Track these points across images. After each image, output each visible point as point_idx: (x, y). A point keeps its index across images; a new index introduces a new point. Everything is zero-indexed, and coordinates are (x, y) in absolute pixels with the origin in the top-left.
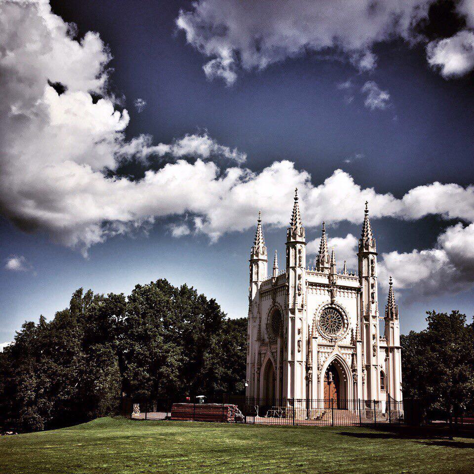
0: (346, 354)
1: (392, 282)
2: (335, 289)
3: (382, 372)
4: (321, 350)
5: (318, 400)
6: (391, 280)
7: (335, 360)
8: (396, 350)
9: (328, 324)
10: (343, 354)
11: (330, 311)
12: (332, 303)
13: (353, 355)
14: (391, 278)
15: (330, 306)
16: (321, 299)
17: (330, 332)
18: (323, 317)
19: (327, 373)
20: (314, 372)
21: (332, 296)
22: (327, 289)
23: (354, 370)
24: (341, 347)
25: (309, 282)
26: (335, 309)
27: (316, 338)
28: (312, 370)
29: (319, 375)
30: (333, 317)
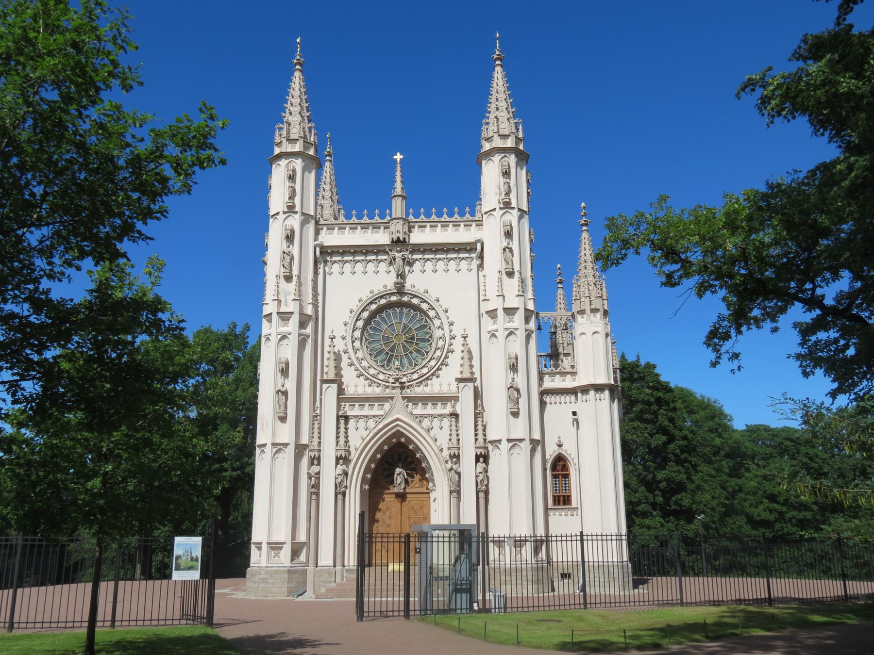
0: (430, 416)
8: (592, 392)
10: (416, 416)
12: (400, 290)
15: (394, 298)
21: (401, 276)
23: (456, 457)
26: (409, 305)
28: (319, 464)
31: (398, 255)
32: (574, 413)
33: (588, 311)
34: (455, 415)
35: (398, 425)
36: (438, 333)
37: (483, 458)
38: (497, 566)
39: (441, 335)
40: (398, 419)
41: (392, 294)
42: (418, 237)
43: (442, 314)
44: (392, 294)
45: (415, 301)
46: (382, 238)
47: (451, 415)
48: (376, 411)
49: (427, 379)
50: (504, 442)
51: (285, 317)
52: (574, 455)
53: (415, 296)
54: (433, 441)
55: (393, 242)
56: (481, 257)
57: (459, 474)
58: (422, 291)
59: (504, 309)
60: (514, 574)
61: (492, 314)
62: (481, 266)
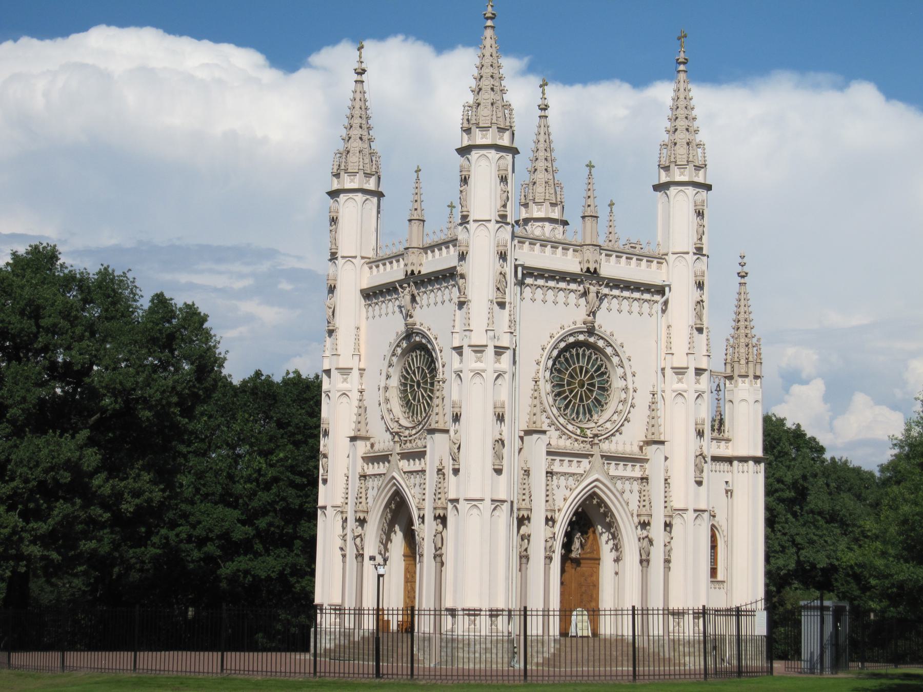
0: (621, 478)
1: (746, 269)
2: (593, 289)
3: (713, 528)
4: (556, 468)
5: (546, 613)
6: (742, 265)
7: (594, 495)
8: (751, 463)
9: (571, 391)
10: (613, 478)
11: (578, 355)
13: (644, 479)
14: (742, 257)
15: (581, 338)
16: (552, 317)
17: (578, 413)
18: (559, 371)
19: (569, 536)
20: (537, 529)
22: (573, 286)
23: (644, 525)
24: (608, 458)
25: (524, 267)
26: (594, 347)
27: (544, 432)
29: (545, 537)
30: (587, 372)
31: (593, 289)
32: (727, 482)
33: (751, 377)
34: (644, 479)
35: (596, 486)
36: (617, 383)
37: (668, 526)
38: (676, 638)
39: (624, 387)
40: (597, 480)
41: (581, 332)
42: (611, 268)
43: (625, 362)
44: (581, 332)
45: (601, 343)
46: (570, 263)
47: (642, 479)
48: (574, 469)
49: (613, 435)
50: (691, 512)
51: (499, 351)
52: (724, 527)
53: (602, 338)
54: (624, 508)
55: (588, 270)
56: (666, 303)
57: (651, 542)
58: (608, 333)
59: (696, 369)
60: (697, 646)
61: (680, 371)
62: (664, 311)
